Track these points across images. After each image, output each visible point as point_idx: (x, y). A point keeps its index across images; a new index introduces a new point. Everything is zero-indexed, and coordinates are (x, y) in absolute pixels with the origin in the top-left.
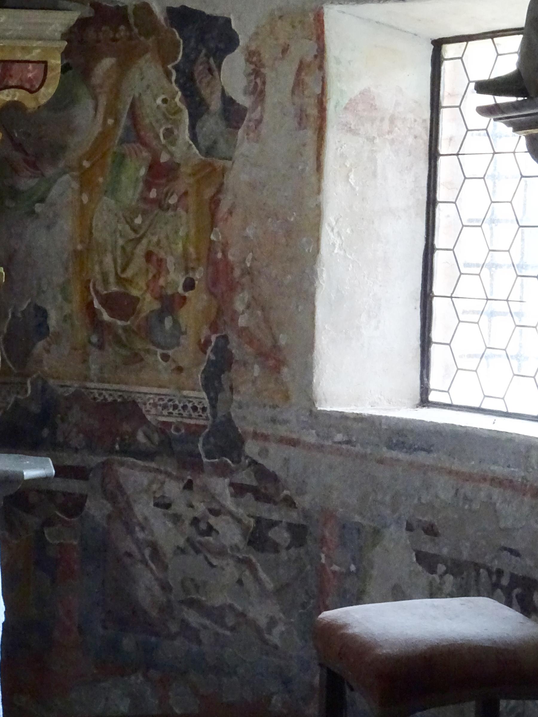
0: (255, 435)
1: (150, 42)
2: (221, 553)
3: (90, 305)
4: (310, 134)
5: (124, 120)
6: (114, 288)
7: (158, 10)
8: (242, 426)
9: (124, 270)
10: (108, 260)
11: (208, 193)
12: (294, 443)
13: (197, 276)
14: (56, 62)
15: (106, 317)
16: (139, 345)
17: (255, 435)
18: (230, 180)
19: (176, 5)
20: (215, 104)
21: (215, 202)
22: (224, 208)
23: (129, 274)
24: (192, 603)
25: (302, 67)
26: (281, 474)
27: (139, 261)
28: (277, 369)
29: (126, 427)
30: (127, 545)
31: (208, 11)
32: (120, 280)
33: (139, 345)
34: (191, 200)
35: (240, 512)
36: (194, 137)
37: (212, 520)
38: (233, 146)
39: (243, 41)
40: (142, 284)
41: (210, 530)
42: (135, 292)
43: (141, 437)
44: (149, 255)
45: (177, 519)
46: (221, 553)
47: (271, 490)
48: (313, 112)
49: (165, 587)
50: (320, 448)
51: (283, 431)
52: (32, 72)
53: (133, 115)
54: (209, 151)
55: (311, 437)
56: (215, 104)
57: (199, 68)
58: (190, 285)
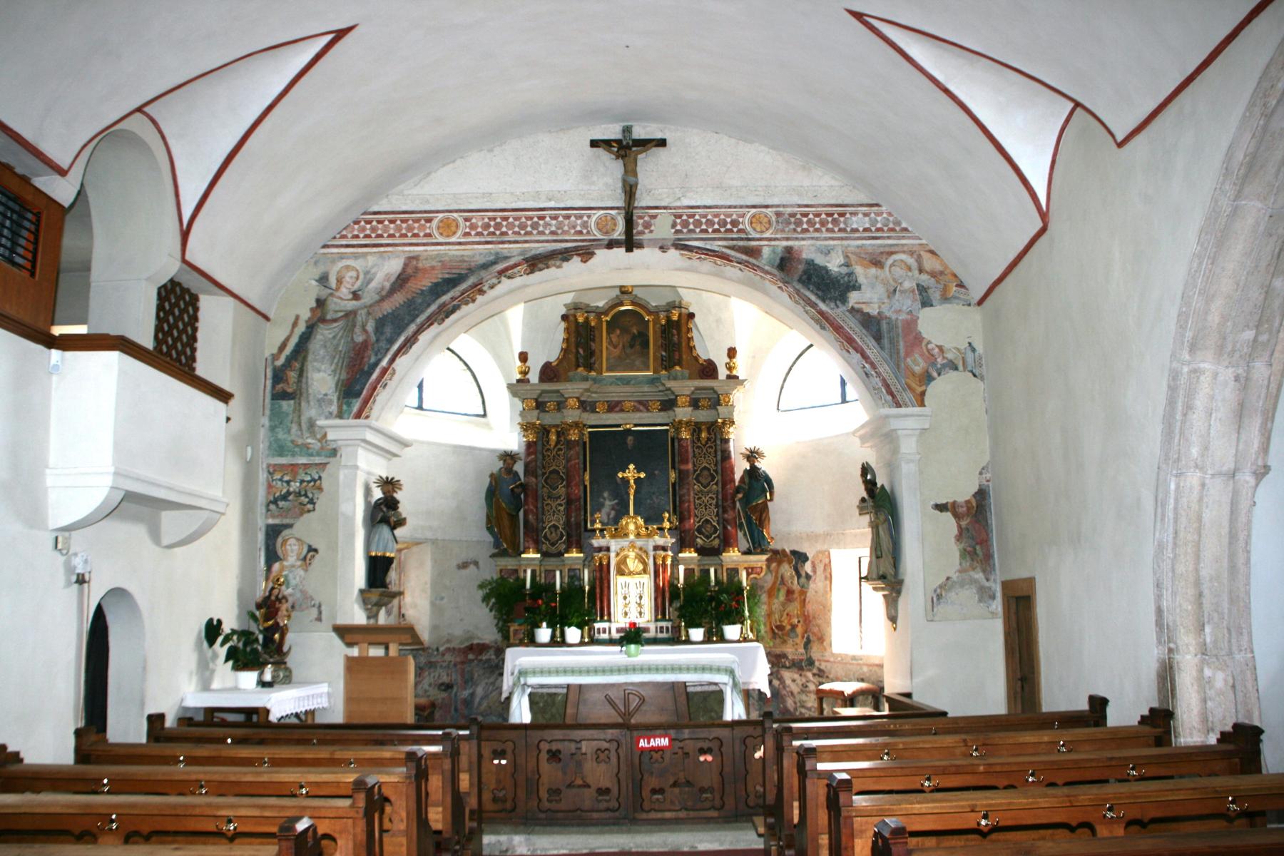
0: (818, 660)
1: (786, 559)
2: (810, 692)
3: (772, 628)
4: (828, 582)
5: (780, 579)
6: (778, 623)
7: (788, 551)
8: (814, 658)
9: (782, 616)
10: (777, 616)
11: (803, 597)
12: (828, 661)
13: (800, 619)
14: (764, 567)
15: (776, 631)
16: (785, 638)
17: (818, 660)
18: (808, 594)
19: (792, 549)
20: (804, 574)
21: (805, 600)
22: (807, 601)
23: (783, 619)
24: (803, 707)
25: (825, 565)
26: (825, 670)
27: (785, 616)
28: (822, 643)
29: (783, 660)
30: (784, 692)
31: (801, 551)
32: (780, 621)
33: (785, 638)
34: (798, 600)
35: (815, 681)
36: (798, 583)
37: (808, 684)
38: (808, 584)
39: (810, 558)
40: (786, 621)
41: (807, 686)
42: (784, 624)
43: (787, 664)
44: (788, 615)
45: (797, 684)
46: (810, 692)
47: (821, 674)
48: (829, 576)
49: (795, 703)
50: (835, 662)
51: (825, 658)
52: (759, 570)
53: (782, 578)
54: (803, 587)
55: (832, 659)
56: (804, 574)
57: (799, 566)
58: (799, 622)
